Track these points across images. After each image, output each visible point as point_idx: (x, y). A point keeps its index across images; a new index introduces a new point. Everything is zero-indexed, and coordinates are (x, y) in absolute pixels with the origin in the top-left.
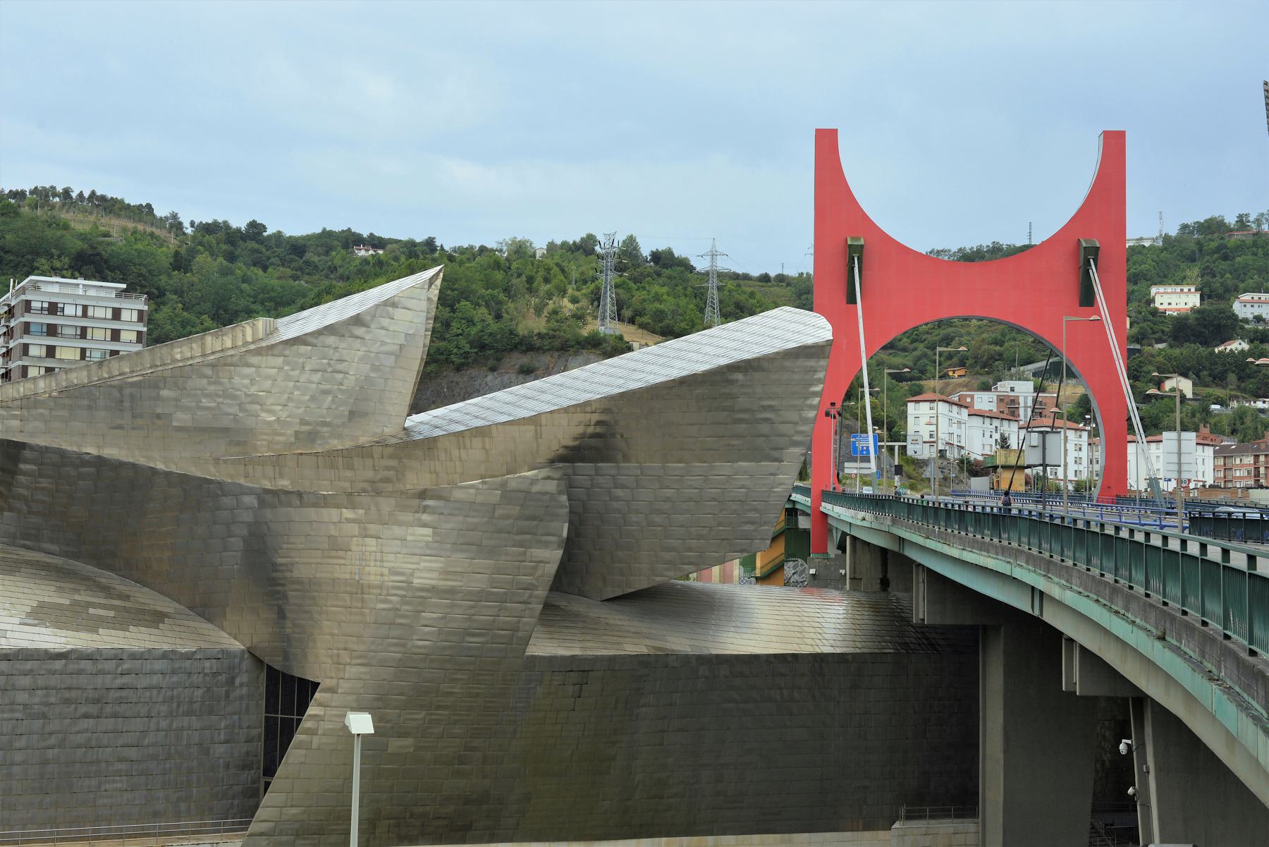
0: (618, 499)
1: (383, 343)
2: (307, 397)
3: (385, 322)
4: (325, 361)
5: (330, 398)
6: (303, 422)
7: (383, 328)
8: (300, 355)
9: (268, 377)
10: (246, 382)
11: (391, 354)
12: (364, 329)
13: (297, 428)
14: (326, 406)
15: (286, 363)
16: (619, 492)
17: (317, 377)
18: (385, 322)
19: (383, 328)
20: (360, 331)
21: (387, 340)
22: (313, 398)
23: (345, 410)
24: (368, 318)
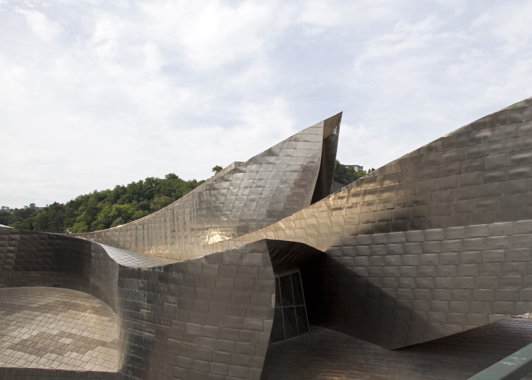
0: (389, 264)
1: (289, 165)
2: (243, 204)
3: (290, 152)
4: (251, 181)
5: (255, 204)
6: (241, 220)
7: (288, 156)
8: (238, 179)
9: (224, 195)
10: (214, 199)
11: (295, 171)
12: (275, 158)
13: (238, 224)
14: (253, 209)
15: (231, 185)
16: (392, 259)
17: (247, 191)
18: (290, 152)
19: (288, 156)
20: (272, 159)
21: (291, 163)
22: (245, 205)
23: (264, 210)
24: (277, 150)
